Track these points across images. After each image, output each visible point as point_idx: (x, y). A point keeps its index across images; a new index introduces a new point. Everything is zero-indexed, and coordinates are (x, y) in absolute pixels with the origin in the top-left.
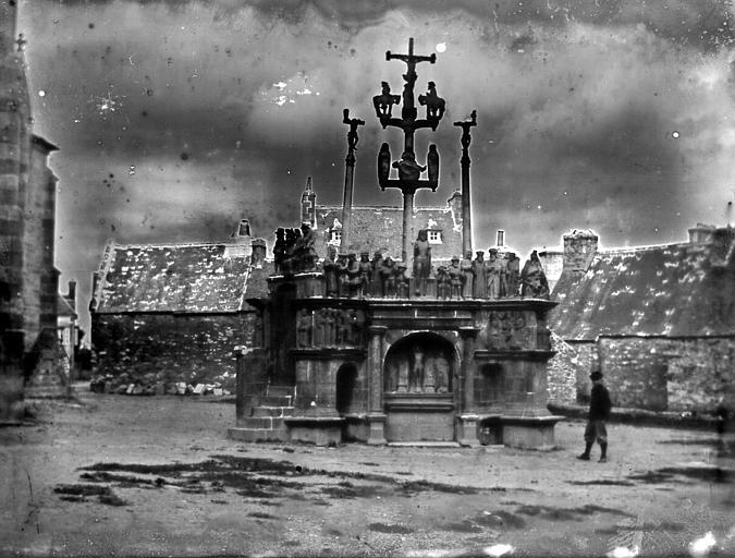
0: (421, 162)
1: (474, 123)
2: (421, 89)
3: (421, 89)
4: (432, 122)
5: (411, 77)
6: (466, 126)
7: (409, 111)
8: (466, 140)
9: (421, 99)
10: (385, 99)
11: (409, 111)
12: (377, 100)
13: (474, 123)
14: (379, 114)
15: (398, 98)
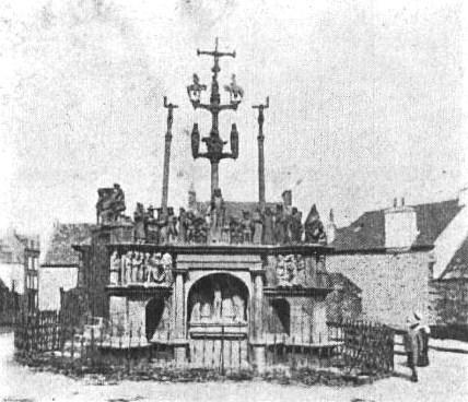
0: (225, 135)
1: (267, 106)
3: (223, 80)
4: (234, 106)
5: (216, 69)
6: (261, 107)
7: (215, 97)
8: (261, 119)
10: (196, 87)
11: (215, 97)
12: (190, 89)
13: (267, 106)
14: (192, 101)
15: (205, 87)
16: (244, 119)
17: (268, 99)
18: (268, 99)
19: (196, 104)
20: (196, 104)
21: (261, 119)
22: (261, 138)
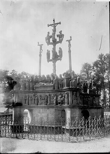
2: (57, 33)
3: (57, 33)
4: (60, 42)
5: (54, 31)
8: (70, 45)
9: (58, 36)
10: (49, 38)
16: (63, 46)
17: (71, 37)
18: (71, 37)
19: (49, 43)
20: (49, 43)
21: (70, 45)
22: (70, 51)
